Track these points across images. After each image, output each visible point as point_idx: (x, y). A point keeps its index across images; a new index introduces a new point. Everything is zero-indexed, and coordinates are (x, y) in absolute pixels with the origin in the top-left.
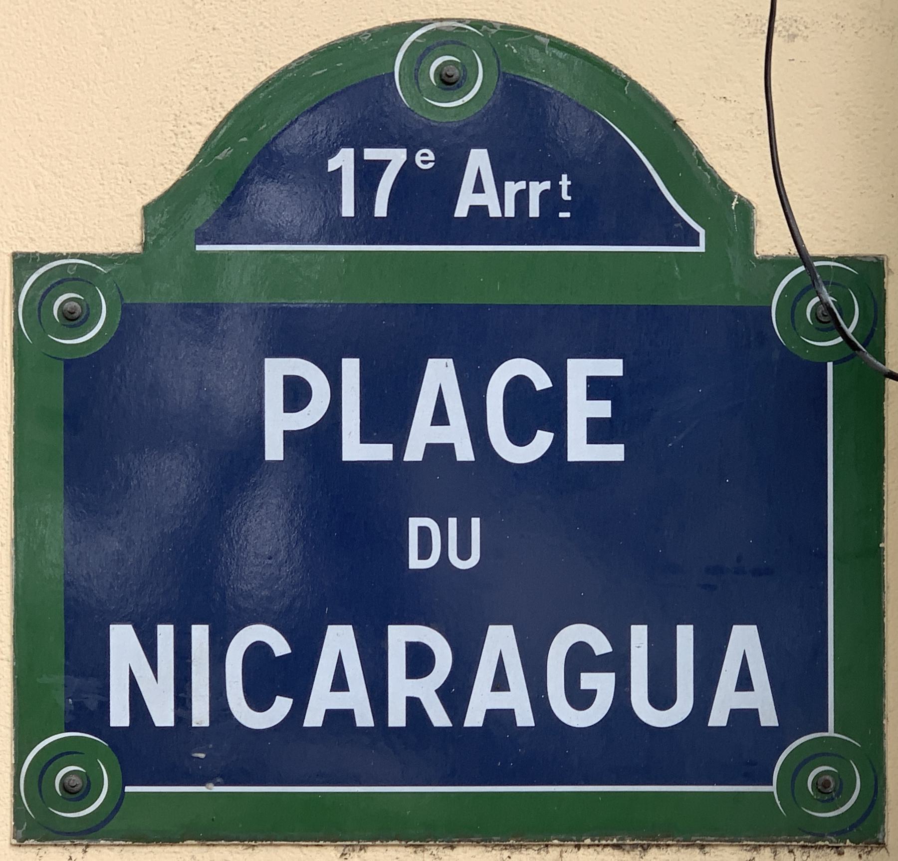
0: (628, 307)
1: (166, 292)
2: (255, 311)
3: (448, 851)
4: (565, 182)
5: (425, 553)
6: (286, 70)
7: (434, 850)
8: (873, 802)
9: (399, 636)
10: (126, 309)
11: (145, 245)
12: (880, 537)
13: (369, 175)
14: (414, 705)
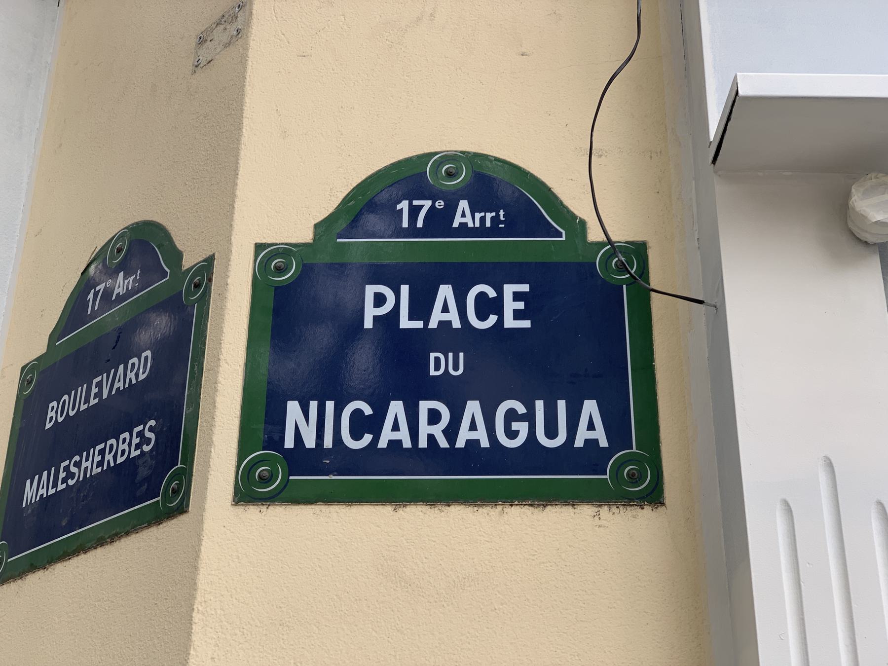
0: (531, 263)
1: (323, 258)
2: (362, 266)
3: (447, 508)
4: (502, 213)
5: (437, 368)
6: (380, 171)
7: (440, 507)
8: (657, 484)
9: (425, 406)
10: (304, 265)
11: (314, 240)
12: (652, 360)
13: (414, 212)
14: (431, 438)
